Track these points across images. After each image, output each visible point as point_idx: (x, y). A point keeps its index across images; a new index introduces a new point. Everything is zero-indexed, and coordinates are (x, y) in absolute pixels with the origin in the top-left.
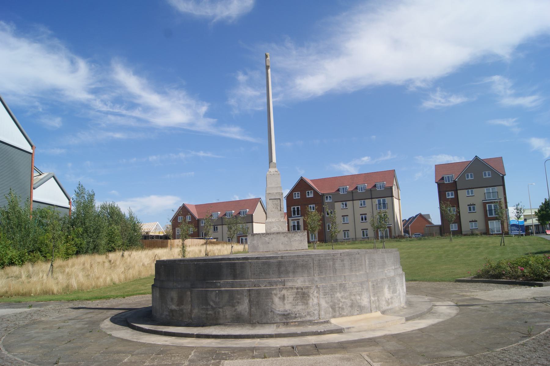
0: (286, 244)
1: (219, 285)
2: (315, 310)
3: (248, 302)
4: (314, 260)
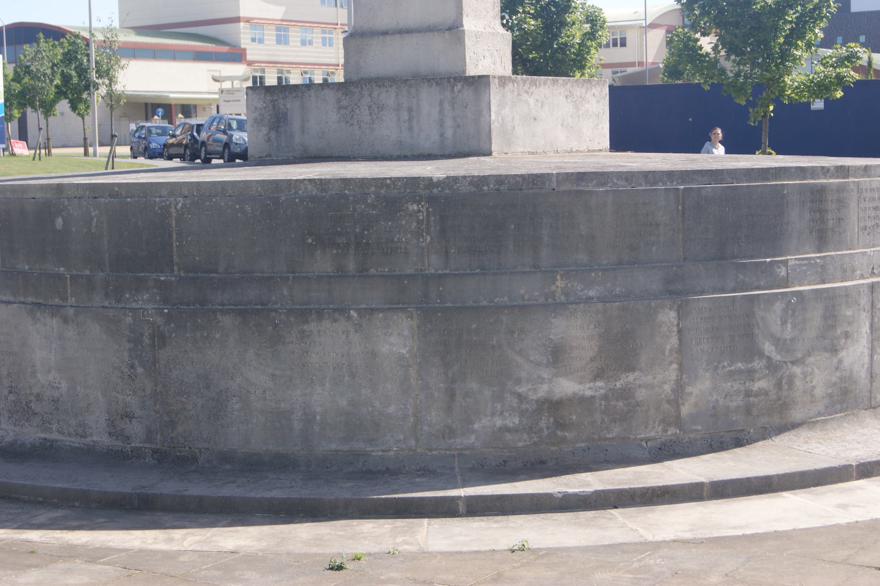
1: (782, 272)
3: (869, 331)
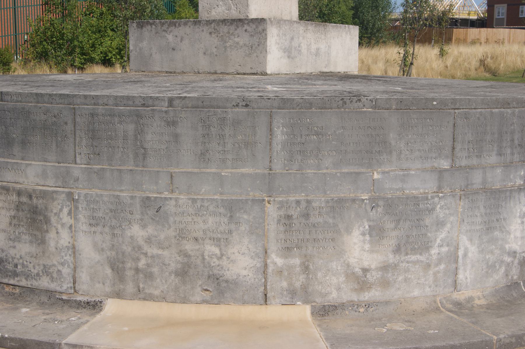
0: (215, 53)
2: (63, 264)
4: (78, 112)
